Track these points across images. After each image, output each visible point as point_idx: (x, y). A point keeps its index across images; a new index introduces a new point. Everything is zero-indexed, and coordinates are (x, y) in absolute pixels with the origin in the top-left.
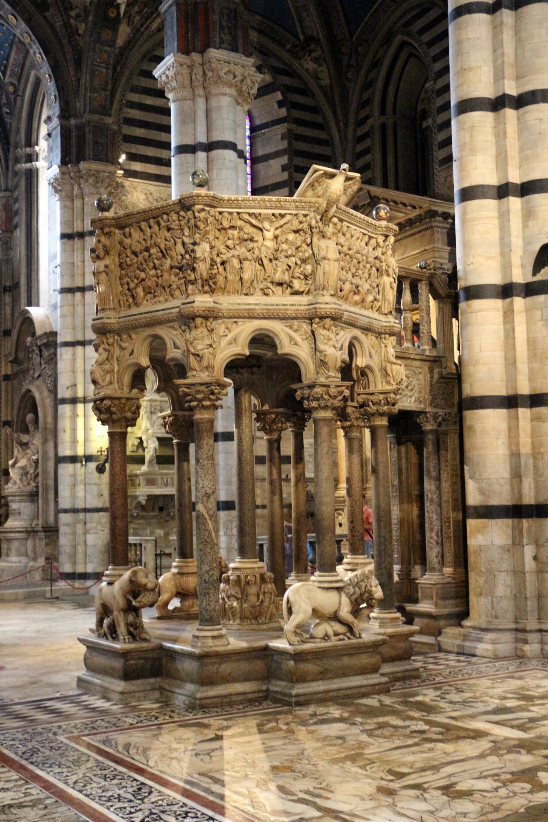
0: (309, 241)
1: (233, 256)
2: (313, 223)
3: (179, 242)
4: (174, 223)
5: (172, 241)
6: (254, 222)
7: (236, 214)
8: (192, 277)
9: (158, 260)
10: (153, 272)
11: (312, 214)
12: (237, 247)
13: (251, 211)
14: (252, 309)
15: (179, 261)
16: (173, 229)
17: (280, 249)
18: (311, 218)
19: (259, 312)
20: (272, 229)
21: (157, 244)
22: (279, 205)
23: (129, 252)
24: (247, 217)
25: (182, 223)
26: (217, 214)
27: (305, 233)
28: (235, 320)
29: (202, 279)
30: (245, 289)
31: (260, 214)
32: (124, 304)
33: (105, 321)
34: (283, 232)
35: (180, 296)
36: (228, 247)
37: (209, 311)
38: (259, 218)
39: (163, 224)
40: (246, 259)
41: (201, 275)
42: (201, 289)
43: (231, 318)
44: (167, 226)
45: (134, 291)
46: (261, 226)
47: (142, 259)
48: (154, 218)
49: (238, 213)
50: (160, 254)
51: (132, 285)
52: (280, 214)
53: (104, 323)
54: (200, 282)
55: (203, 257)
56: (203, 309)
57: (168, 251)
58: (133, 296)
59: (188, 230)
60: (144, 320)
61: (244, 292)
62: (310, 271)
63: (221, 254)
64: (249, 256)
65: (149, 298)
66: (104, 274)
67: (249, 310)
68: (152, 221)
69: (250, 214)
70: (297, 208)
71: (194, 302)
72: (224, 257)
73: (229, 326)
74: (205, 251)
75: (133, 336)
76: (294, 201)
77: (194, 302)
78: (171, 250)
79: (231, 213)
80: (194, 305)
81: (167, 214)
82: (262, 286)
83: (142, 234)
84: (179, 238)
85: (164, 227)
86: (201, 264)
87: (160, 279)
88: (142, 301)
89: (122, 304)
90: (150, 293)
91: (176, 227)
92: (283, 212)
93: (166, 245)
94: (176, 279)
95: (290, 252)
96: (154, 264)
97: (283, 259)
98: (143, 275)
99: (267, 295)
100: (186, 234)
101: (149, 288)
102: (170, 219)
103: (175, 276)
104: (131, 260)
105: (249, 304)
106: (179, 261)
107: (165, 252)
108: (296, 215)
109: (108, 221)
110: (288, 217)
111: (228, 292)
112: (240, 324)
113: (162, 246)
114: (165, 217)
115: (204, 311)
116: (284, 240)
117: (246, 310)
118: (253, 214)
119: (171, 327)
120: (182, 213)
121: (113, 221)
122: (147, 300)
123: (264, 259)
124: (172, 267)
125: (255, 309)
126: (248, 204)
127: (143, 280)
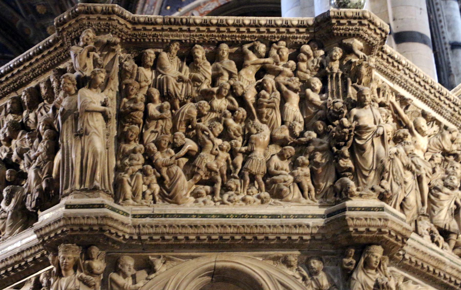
3: (295, 98)
4: (282, 63)
5: (278, 93)
9: (235, 120)
10: (219, 142)
15: (297, 131)
16: (280, 73)
19: (449, 270)
21: (240, 91)
22: (437, 100)
23: (156, 93)
25: (303, 65)
28: (407, 275)
32: (134, 193)
33: (106, 211)
35: (303, 200)
39: (253, 58)
43: (406, 268)
44: (264, 63)
45: (164, 170)
46: (411, 124)
47: (195, 113)
48: (231, 44)
50: (242, 112)
51: (160, 157)
53: (105, 217)
56: (399, 229)
57: (265, 110)
58: (161, 181)
60: (216, 230)
65: (203, 192)
66: (100, 117)
68: (225, 47)
73: (401, 283)
75: (159, 265)
78: (274, 108)
81: (270, 45)
83: (186, 68)
84: (295, 91)
85: (254, 64)
87: (240, 159)
88: (186, 195)
89: (128, 189)
90: (211, 182)
93: (258, 97)
94: (286, 165)
96: (226, 126)
98: (191, 145)
99: (437, 244)
101: (209, 169)
102: (274, 52)
104: (161, 109)
106: (297, 131)
107: (254, 110)
109: (122, 21)
112: (410, 284)
113: (251, 97)
114: (262, 48)
115: (398, 233)
119: (276, 259)
121: (130, 26)
122: (196, 195)
124: (273, 140)
126: (407, 77)
127: (189, 155)
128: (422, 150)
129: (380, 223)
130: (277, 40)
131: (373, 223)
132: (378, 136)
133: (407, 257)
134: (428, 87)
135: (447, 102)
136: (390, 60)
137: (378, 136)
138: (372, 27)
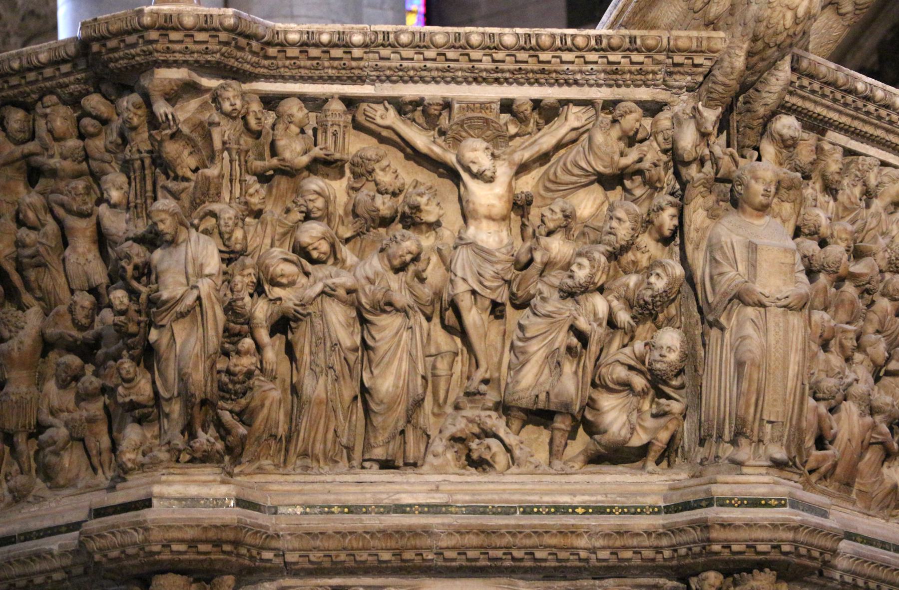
0: (667, 219)
1: (327, 293)
2: (688, 139)
6: (421, 140)
7: (337, 106)
8: (143, 389)
11: (682, 103)
12: (346, 252)
13: (410, 91)
14: (414, 532)
17: (538, 256)
18: (677, 121)
20: (503, 172)
22: (533, 65)
24: (389, 118)
25: (97, 145)
26: (256, 107)
27: (653, 185)
29: (186, 396)
30: (381, 439)
31: (447, 105)
34: (552, 185)
36: (302, 251)
37: (217, 543)
38: (444, 122)
40: (387, 306)
41: (183, 378)
42: (179, 441)
46: (451, 158)
49: (350, 102)
52: (537, 104)
54: (175, 409)
55: (190, 300)
56: (190, 534)
59: (122, 179)
61: (379, 453)
62: (673, 357)
63: (274, 283)
64: (402, 298)
67: (400, 532)
69: (401, 107)
70: (614, 75)
71: (146, 503)
72: (289, 297)
74: (200, 275)
76: (601, 46)
77: (146, 503)
79: (316, 104)
80: (148, 515)
82: (459, 425)
86: (180, 330)
91: (68, 165)
92: (550, 93)
95: (581, 274)
97: (554, 304)
100: (115, 195)
103: (63, 385)
105: (400, 509)
108: (610, 105)
110: (575, 118)
111: (305, 454)
115: (192, 543)
116: (554, 219)
117: (386, 533)
118: (418, 103)
120: (95, 102)
123: (465, 302)
125: (427, 531)
128: (490, 218)
129: (138, 537)
130: (35, 96)
131: (127, 539)
132: (182, 315)
133: (291, 557)
134: (475, 55)
135: (567, 56)
136: (314, 52)
137: (182, 315)
138: (174, 36)
